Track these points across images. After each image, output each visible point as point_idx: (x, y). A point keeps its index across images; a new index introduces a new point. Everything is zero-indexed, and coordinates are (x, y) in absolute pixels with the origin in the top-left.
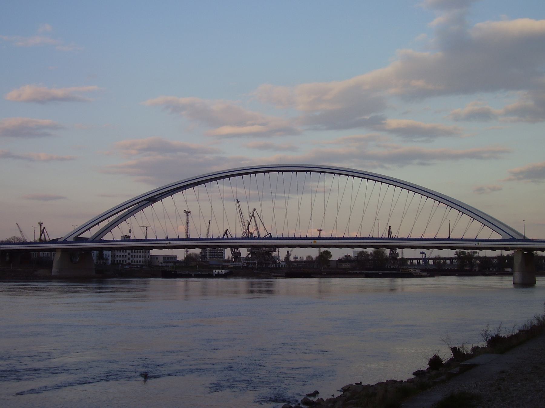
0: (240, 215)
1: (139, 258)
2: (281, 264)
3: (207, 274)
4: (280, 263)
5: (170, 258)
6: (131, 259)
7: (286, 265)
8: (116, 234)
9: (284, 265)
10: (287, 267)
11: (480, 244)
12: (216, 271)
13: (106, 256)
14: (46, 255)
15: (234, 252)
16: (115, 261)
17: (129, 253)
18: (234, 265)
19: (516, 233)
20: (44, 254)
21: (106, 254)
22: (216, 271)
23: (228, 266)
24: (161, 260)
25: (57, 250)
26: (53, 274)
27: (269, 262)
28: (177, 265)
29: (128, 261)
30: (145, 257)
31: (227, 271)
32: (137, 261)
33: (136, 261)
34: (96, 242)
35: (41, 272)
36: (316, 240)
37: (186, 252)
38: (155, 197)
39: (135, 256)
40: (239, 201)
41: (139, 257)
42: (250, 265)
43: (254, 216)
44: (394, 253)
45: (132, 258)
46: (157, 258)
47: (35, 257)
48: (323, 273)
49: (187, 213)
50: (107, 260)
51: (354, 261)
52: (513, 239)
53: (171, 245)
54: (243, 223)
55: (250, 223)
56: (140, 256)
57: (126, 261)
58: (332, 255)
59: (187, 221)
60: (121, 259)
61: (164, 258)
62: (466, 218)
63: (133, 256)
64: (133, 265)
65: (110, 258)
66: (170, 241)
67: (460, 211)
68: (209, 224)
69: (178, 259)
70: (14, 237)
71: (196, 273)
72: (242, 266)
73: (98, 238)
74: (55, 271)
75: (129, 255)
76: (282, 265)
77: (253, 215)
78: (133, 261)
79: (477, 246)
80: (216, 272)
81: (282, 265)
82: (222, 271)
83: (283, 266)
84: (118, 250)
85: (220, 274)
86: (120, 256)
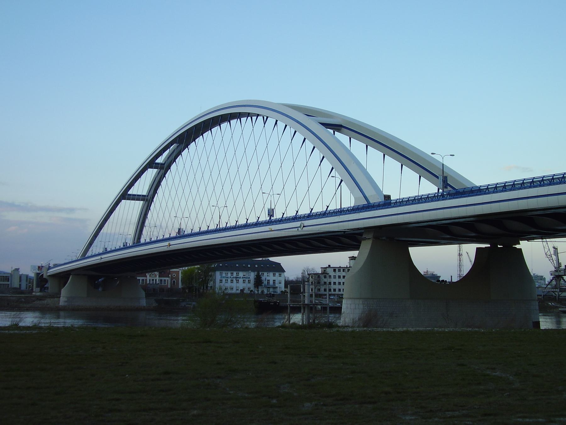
14: (157, 280)
20: (153, 280)
74: (62, 301)
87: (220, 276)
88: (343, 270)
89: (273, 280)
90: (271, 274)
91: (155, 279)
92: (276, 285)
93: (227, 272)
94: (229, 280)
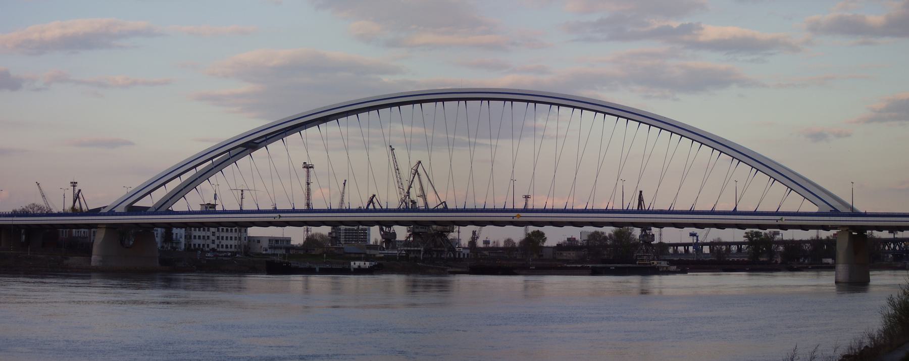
0: (396, 172)
1: (229, 241)
2: (462, 252)
3: (341, 267)
4: (461, 250)
6: (217, 242)
7: (471, 254)
8: (192, 201)
9: (468, 254)
10: (473, 257)
11: (783, 220)
12: (355, 264)
13: (177, 236)
14: (82, 232)
15: (386, 233)
16: (191, 244)
17: (213, 232)
18: (386, 255)
19: (840, 203)
20: (78, 232)
21: (177, 234)
22: (355, 264)
23: (374, 255)
24: (265, 244)
25: (99, 226)
26: (93, 264)
27: (443, 249)
28: (291, 252)
29: (212, 246)
30: (240, 238)
31: (373, 263)
32: (227, 246)
33: (224, 246)
34: (161, 214)
35: (74, 260)
36: (520, 214)
37: (306, 232)
38: (256, 141)
39: (223, 237)
40: (394, 149)
41: (229, 238)
42: (412, 253)
43: (418, 174)
44: (646, 235)
45: (218, 241)
46: (259, 242)
47: (66, 236)
48: (531, 268)
49: (308, 168)
50: (178, 243)
51: (581, 248)
52: (835, 213)
53: (282, 219)
54: (400, 184)
55: (411, 184)
56: (231, 237)
58: (546, 238)
59: (308, 180)
60: (201, 242)
61: (269, 240)
62: (762, 178)
63: (220, 238)
64: (220, 252)
65: (183, 240)
66: (281, 214)
67: (753, 167)
68: (344, 185)
69: (292, 243)
70: (34, 204)
71: (322, 267)
72: (399, 256)
73: (163, 207)
74: (96, 259)
75: (213, 235)
76: (464, 254)
77: (417, 171)
78: (220, 246)
79: (780, 222)
80: (355, 264)
81: (464, 254)
82: (365, 264)
83: (466, 256)
84: (195, 227)
85: (364, 269)
86: (199, 237)
92: (181, 239)
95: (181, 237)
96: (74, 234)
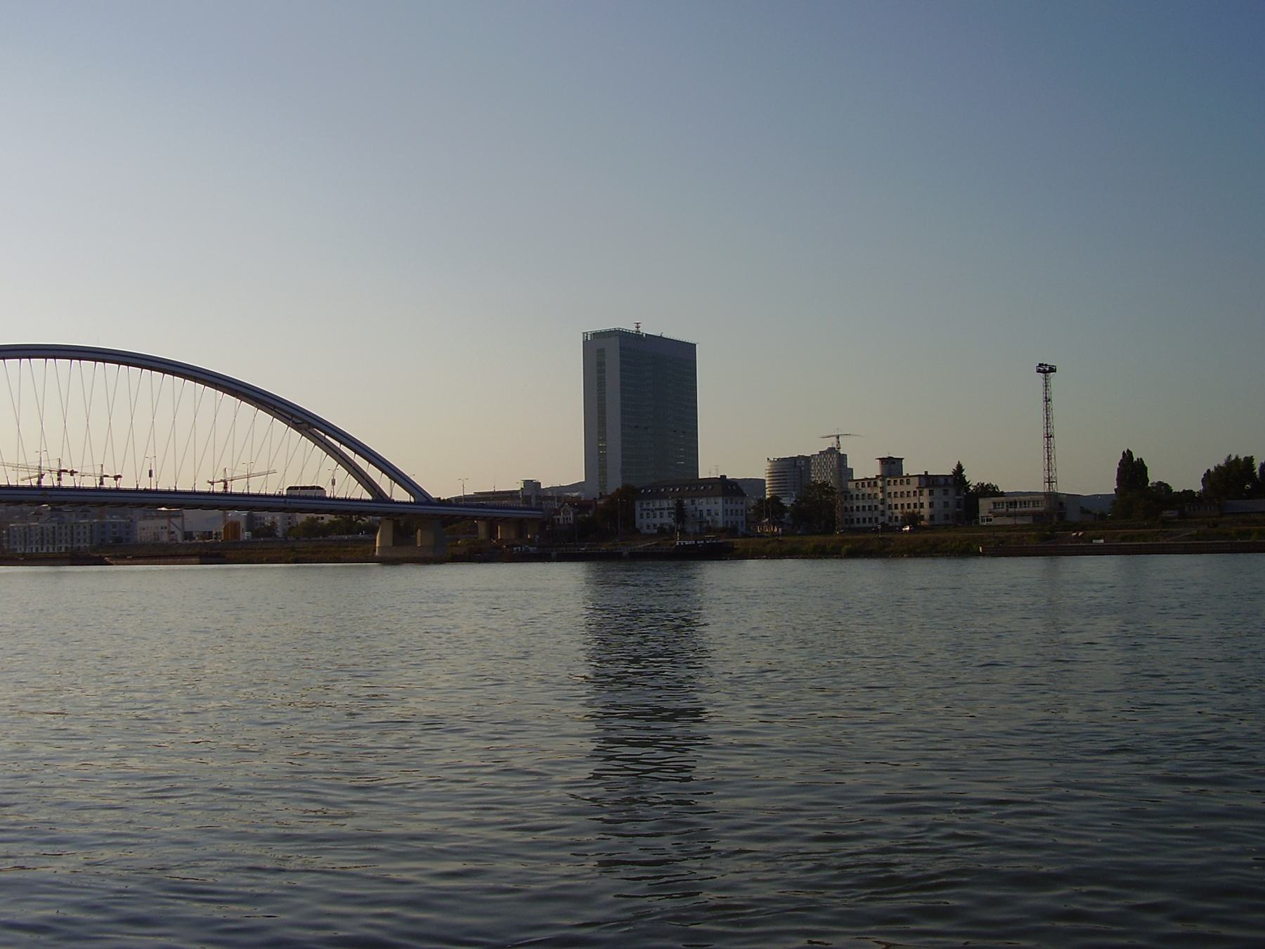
5: (1020, 502)
6: (888, 513)
20: (567, 519)
29: (881, 520)
39: (896, 505)
57: (876, 519)
60: (867, 515)
63: (893, 507)
87: (639, 509)
88: (868, 483)
89: (708, 510)
90: (704, 500)
91: (568, 516)
93: (648, 502)
94: (651, 514)
95: (717, 514)
96: (786, 514)
